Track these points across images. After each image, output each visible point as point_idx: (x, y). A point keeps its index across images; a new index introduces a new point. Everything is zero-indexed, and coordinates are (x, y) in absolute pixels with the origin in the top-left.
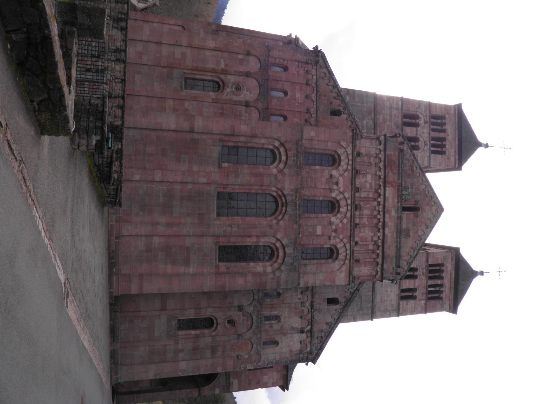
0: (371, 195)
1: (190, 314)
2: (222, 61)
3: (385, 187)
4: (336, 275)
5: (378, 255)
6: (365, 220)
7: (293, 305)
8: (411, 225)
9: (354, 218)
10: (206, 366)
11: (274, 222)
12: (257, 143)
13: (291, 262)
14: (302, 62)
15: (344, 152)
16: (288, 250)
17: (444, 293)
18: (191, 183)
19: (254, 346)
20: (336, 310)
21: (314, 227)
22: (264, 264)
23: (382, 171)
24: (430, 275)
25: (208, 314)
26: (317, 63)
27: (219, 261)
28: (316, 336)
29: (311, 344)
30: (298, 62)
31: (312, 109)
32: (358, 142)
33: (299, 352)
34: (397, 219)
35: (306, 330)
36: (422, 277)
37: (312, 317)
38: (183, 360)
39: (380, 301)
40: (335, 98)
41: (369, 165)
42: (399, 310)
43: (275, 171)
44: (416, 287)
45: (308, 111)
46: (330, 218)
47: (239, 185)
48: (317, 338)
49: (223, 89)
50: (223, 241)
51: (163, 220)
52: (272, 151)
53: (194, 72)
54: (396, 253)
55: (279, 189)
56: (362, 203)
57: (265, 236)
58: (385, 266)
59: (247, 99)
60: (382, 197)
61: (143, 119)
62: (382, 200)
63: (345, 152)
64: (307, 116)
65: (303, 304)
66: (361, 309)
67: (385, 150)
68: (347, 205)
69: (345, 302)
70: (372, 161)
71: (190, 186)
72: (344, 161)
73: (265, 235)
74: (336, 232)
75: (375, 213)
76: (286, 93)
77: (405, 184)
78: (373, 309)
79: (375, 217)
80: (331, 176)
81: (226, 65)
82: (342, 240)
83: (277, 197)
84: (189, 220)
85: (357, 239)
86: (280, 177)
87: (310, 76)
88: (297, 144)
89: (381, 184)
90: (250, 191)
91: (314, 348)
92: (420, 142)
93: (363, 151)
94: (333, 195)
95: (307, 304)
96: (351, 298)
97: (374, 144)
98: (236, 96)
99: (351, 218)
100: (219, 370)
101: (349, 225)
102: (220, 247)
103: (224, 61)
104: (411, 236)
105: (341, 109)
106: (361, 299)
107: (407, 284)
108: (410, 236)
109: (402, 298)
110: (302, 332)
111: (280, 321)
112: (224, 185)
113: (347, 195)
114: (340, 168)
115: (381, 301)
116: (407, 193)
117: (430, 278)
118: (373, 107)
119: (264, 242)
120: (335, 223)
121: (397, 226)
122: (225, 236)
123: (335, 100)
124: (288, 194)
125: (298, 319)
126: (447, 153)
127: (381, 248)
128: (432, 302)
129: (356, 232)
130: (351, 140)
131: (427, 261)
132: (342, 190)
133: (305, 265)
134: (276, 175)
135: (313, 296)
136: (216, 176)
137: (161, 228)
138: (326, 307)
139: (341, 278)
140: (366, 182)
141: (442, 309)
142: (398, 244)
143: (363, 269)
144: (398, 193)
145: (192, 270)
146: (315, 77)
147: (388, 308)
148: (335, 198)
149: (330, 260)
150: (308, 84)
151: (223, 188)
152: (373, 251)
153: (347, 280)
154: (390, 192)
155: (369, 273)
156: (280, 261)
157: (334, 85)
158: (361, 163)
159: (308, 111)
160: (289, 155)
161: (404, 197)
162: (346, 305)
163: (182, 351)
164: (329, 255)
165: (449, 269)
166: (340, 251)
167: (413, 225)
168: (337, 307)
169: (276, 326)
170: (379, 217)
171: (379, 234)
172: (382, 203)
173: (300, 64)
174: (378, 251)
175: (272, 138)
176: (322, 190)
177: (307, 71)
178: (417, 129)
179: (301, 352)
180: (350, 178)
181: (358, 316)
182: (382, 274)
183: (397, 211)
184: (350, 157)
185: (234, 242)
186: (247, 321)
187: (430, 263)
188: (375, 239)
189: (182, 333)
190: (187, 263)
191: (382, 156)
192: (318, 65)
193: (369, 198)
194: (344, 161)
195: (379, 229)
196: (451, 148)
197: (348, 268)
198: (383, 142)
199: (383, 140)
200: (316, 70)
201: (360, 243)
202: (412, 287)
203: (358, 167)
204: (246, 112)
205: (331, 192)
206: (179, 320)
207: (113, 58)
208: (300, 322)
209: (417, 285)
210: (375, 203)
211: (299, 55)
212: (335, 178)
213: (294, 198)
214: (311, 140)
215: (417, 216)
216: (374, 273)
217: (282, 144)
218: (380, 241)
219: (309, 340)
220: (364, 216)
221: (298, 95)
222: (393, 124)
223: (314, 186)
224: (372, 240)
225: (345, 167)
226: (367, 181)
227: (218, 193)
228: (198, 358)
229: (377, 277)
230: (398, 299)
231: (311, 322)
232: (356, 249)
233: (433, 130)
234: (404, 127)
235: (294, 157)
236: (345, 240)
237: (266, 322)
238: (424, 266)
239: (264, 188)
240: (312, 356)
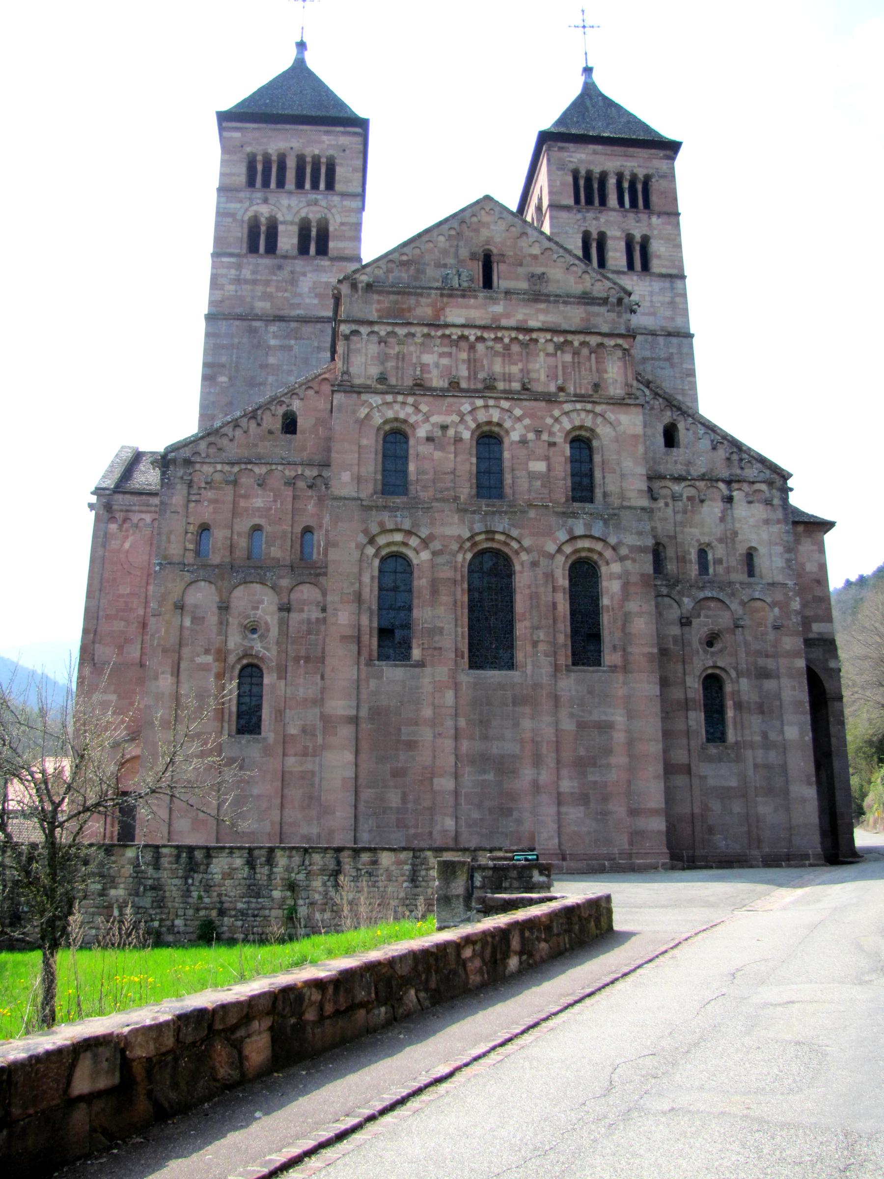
0: (464, 355)
1: (697, 719)
2: (200, 660)
3: (447, 326)
4: (624, 432)
5: (583, 344)
6: (515, 369)
7: (679, 517)
8: (521, 270)
9: (510, 392)
10: (793, 688)
11: (524, 556)
12: (371, 590)
13: (601, 523)
14: (189, 494)
15: (379, 411)
16: (579, 530)
17: (635, 171)
18: (456, 721)
19: (757, 595)
20: (688, 430)
21: (532, 476)
22: (604, 577)
23: (413, 330)
24: (597, 202)
25: (696, 686)
26: (188, 462)
27: (600, 665)
28: (739, 471)
29: (753, 483)
30: (189, 501)
31: (287, 472)
32: (357, 381)
33: (769, 506)
34: (511, 300)
35: (726, 492)
36: (602, 220)
37: (702, 478)
38: (782, 732)
39: (652, 318)
40: (259, 425)
41: (403, 360)
42: (671, 276)
43: (425, 555)
44: (624, 235)
45: (291, 483)
46: (512, 443)
47: (456, 626)
48: (742, 468)
49: (256, 657)
50: (564, 657)
51: (527, 773)
52: (383, 560)
53: (226, 717)
54: (578, 303)
55: (461, 548)
56: (481, 376)
57: (553, 576)
58: (605, 329)
59: (274, 608)
60: (466, 332)
61: (338, 814)
62: (473, 331)
63: (380, 410)
64: (301, 484)
65: (675, 498)
66: (669, 359)
67: (371, 323)
68: (486, 407)
69: (672, 410)
70: (394, 350)
71: (462, 723)
72: (397, 412)
73: (550, 576)
74: (541, 431)
75: (499, 347)
76: (257, 528)
77: (438, 281)
78: (670, 334)
79: (507, 348)
80: (430, 439)
81: (207, 652)
82: (557, 420)
83: (475, 550)
84: (527, 724)
85: (553, 388)
86: (436, 545)
87: (218, 477)
88: (369, 508)
89: (439, 333)
90: (466, 604)
91: (762, 477)
92: (311, 216)
93: (375, 371)
94: (466, 435)
95: (676, 488)
96: (664, 398)
97: (359, 346)
98: (268, 631)
99: (513, 399)
100: (801, 663)
101: (526, 403)
102: (574, 664)
103: (198, 656)
104: (543, 270)
105: (281, 410)
106: (648, 359)
107: (616, 256)
108: (544, 274)
109: (646, 267)
110: (729, 500)
111: (709, 545)
112: (456, 656)
113: (466, 407)
114: (412, 420)
115: (654, 314)
116: (456, 277)
117: (603, 202)
118: (237, 323)
119: (564, 578)
120: (524, 432)
121: (523, 300)
122: (555, 653)
123: (264, 424)
124: (471, 529)
125: (705, 508)
126: (331, 152)
127: (570, 337)
128: (654, 199)
129: (540, 388)
130: (355, 395)
131: (567, 208)
132: (457, 419)
133: (605, 495)
134: (434, 554)
135: (662, 477)
136: (439, 672)
137: (545, 777)
138: (681, 450)
139: (631, 422)
140: (437, 365)
141: (670, 176)
142: (561, 300)
143: (610, 375)
144: (457, 296)
145: (619, 718)
146: (219, 467)
147: (667, 299)
148: (473, 433)
149: (595, 443)
150: (235, 483)
151: (463, 658)
152: (576, 353)
153: (634, 410)
154: (456, 314)
155: (619, 364)
156: (599, 546)
157: (232, 425)
158: (400, 375)
159: (291, 483)
160: (392, 527)
161: (465, 284)
162: (679, 409)
163: (765, 735)
164: (583, 445)
165: (583, 156)
166: (577, 423)
167: (521, 265)
168: (681, 426)
169: (718, 552)
170: (507, 340)
171: (542, 341)
172: (479, 333)
173: (194, 498)
174: (576, 344)
175: (360, 561)
176: (458, 459)
177: (207, 483)
178: (284, 223)
179: (768, 503)
180: (431, 399)
181: (685, 366)
182: (620, 336)
183: (494, 300)
184: (389, 398)
185: (565, 635)
186: (709, 608)
187: (571, 201)
188: (550, 348)
189: (731, 736)
190: (605, 727)
191: (383, 331)
192: (193, 459)
193: (469, 360)
194: (397, 412)
195: (531, 340)
196: (319, 143)
197: (611, 407)
198: (354, 327)
199: (348, 326)
200: (203, 463)
201: (560, 382)
202: (623, 244)
203: (409, 382)
204: (302, 610)
205: (461, 440)
206: (708, 740)
207: (266, 870)
208: (710, 502)
209: (618, 234)
210: (480, 347)
211: (174, 501)
212: (431, 431)
213: (477, 517)
214: (359, 479)
215: (503, 255)
216: (619, 353)
217: (372, 541)
218: (555, 339)
219: (745, 486)
220: (507, 370)
221: (258, 502)
222: (274, 278)
223: (452, 476)
224: (555, 355)
225: (409, 410)
226: (434, 362)
227: (470, 667)
228: (778, 703)
229: (626, 346)
230: (648, 278)
231: (710, 479)
232: (571, 389)
233: (281, 184)
234: (278, 252)
235: (396, 517)
236: (557, 413)
237: (711, 571)
238: (579, 216)
239: (459, 578)
240: (778, 478)
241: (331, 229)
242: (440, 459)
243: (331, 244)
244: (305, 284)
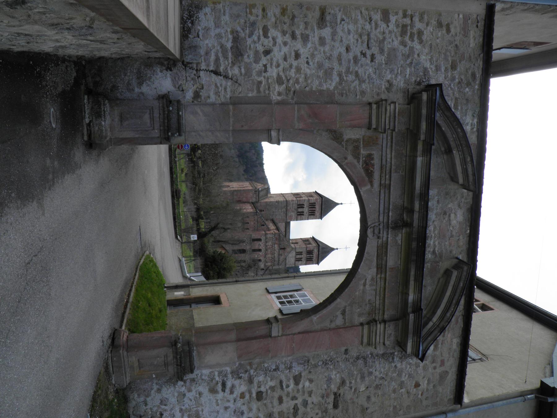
63: (263, 238)
128: (308, 262)
141: (313, 264)
154: (276, 246)
196: (318, 213)
241: (302, 216)
242: (256, 245)
243: (299, 217)
244: (293, 214)
